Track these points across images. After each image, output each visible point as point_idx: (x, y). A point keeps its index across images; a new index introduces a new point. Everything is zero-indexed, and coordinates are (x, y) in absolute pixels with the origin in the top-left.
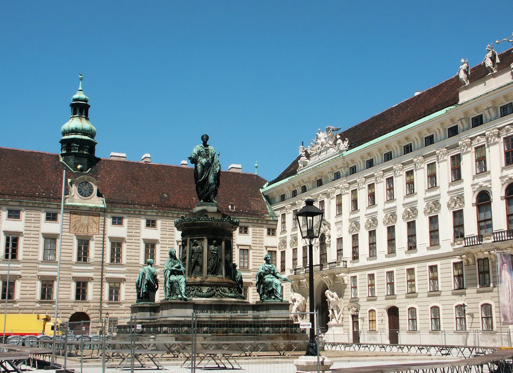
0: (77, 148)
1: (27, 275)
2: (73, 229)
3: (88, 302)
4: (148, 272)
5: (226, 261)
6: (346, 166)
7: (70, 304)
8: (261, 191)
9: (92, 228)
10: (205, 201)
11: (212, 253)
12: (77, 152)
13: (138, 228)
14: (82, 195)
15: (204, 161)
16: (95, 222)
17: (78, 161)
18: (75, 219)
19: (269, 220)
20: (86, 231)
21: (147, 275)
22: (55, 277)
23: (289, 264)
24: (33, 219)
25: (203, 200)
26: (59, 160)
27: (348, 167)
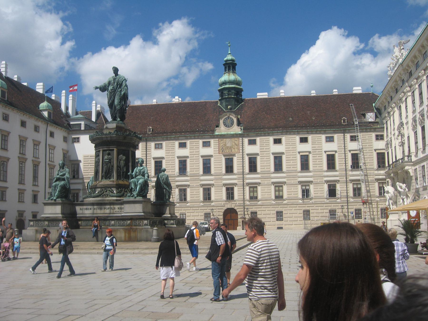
1: (193, 184)
3: (235, 201)
5: (119, 167)
6: (406, 72)
7: (223, 203)
8: (374, 104)
9: (234, 149)
11: (105, 162)
12: (227, 97)
13: (268, 145)
14: (226, 126)
15: (110, 88)
16: (237, 145)
17: (228, 104)
18: (222, 144)
19: (376, 128)
23: (391, 163)
24: (194, 147)
26: (218, 104)
27: (408, 72)
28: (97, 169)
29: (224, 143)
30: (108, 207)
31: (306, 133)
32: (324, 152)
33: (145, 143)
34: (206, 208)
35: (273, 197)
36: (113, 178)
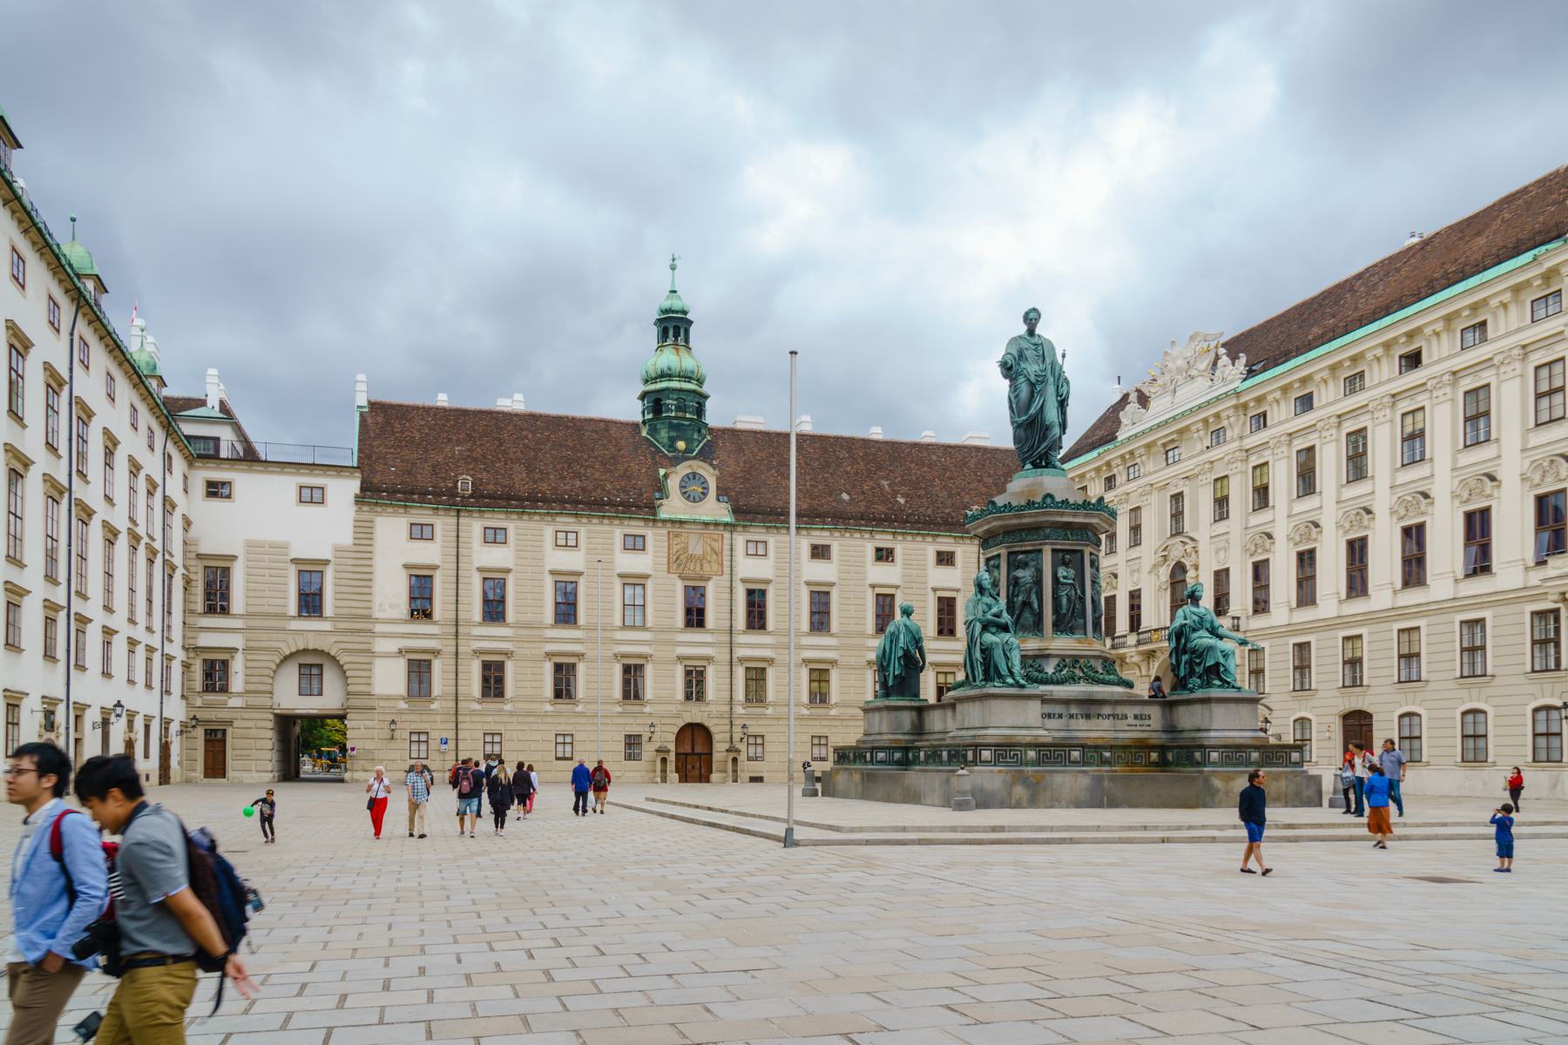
0: (673, 407)
2: (675, 565)
4: (904, 630)
9: (710, 562)
10: (1036, 466)
12: (673, 414)
14: (688, 498)
17: (674, 434)
18: (678, 547)
20: (698, 569)
21: (902, 636)
22: (645, 657)
25: (1032, 463)
26: (640, 432)
28: (1026, 604)
29: (683, 545)
30: (1107, 710)
31: (891, 537)
32: (930, 590)
33: (454, 520)
34: (631, 721)
35: (805, 698)
36: (1082, 632)
